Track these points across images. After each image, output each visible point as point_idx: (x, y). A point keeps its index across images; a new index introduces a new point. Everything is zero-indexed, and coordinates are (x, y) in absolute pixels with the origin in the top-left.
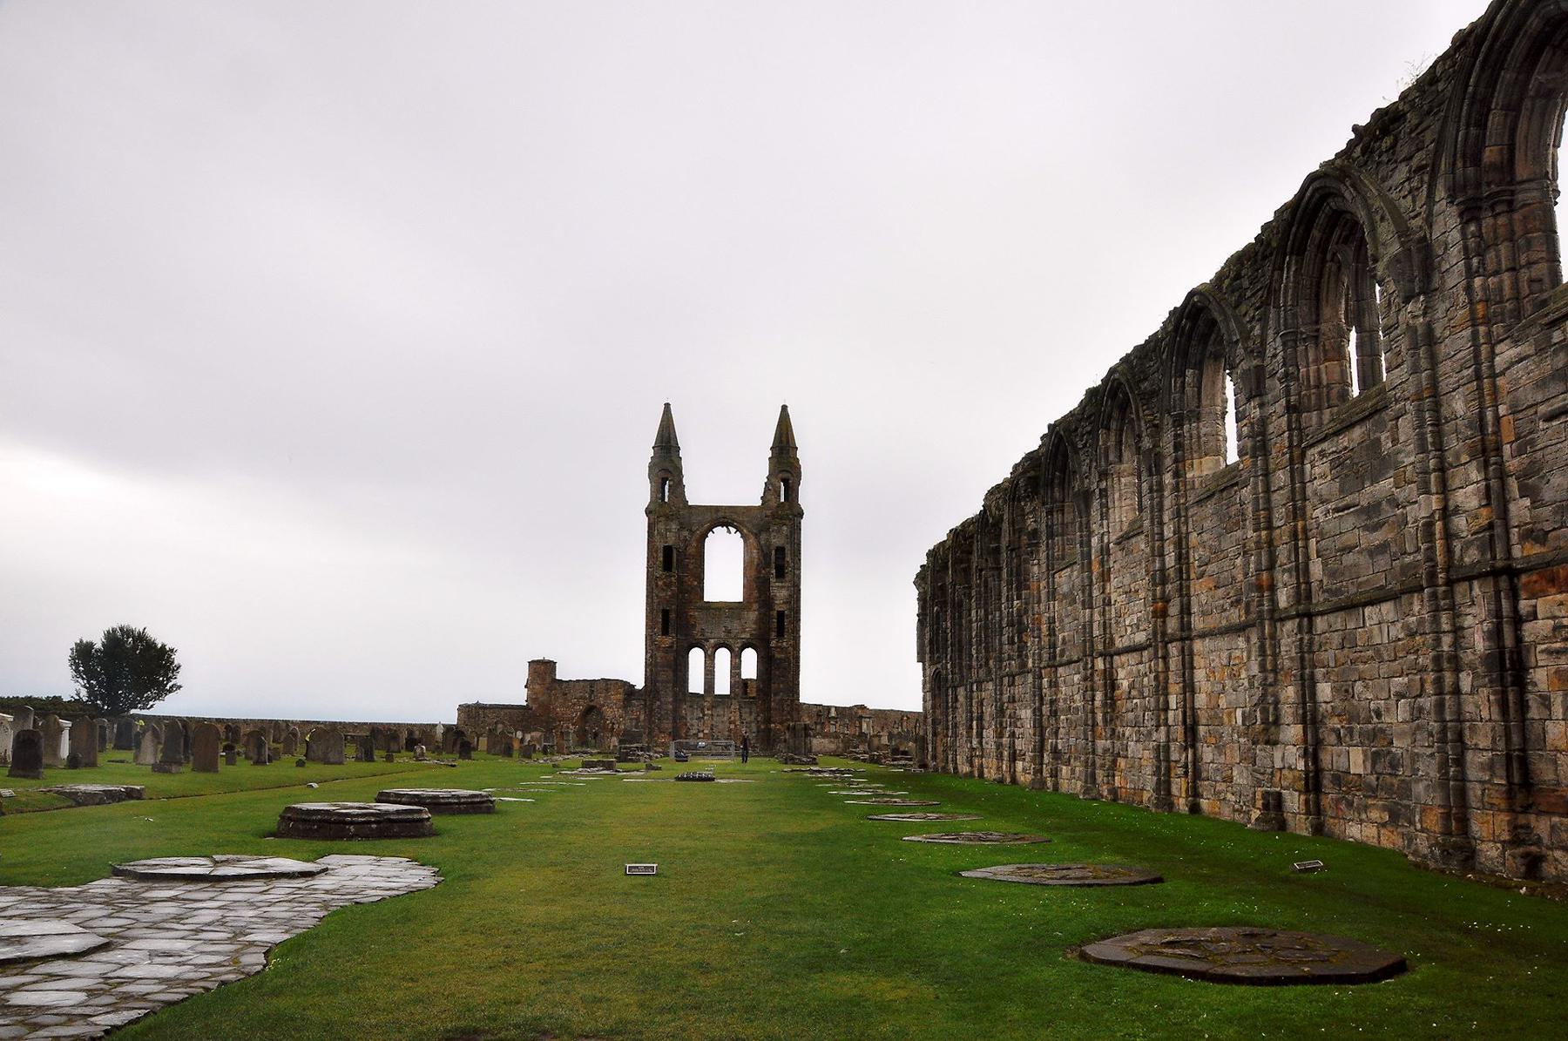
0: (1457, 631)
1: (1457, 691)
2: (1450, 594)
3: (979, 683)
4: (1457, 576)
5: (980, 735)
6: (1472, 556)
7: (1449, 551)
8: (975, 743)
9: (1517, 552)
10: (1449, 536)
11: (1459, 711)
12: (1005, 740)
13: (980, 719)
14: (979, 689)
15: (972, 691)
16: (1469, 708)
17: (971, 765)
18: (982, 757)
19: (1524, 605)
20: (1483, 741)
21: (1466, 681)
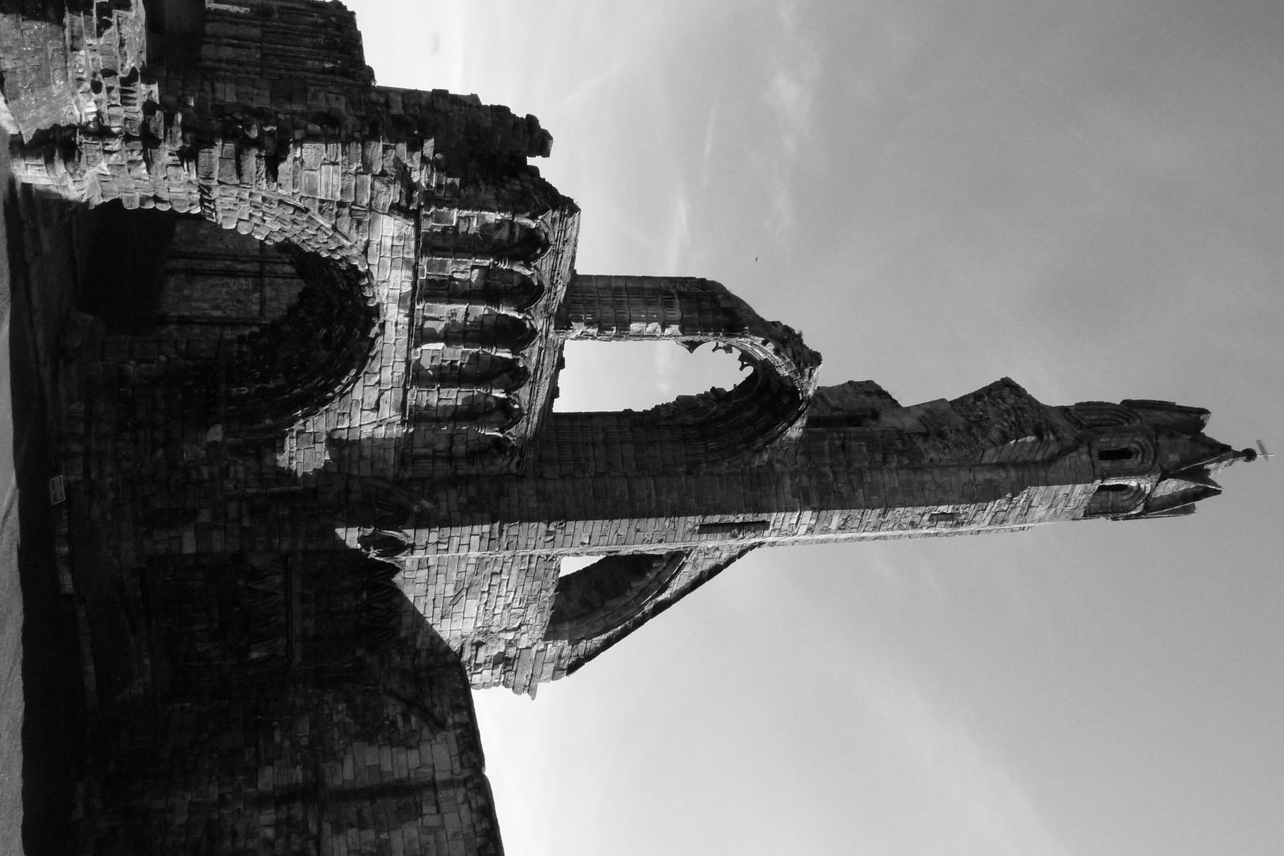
0: (245, 262)
1: (226, 260)
2: (257, 261)
3: (261, 48)
4: (262, 264)
5: (229, 45)
6: (268, 268)
7: (272, 262)
8: (224, 40)
9: (267, 279)
10: (276, 263)
11: (218, 260)
12: (224, 65)
13: (239, 46)
14: (257, 48)
15: (256, 42)
16: (219, 262)
17: (211, 36)
18: (216, 45)
19: (250, 279)
20: (208, 265)
21: (228, 263)
